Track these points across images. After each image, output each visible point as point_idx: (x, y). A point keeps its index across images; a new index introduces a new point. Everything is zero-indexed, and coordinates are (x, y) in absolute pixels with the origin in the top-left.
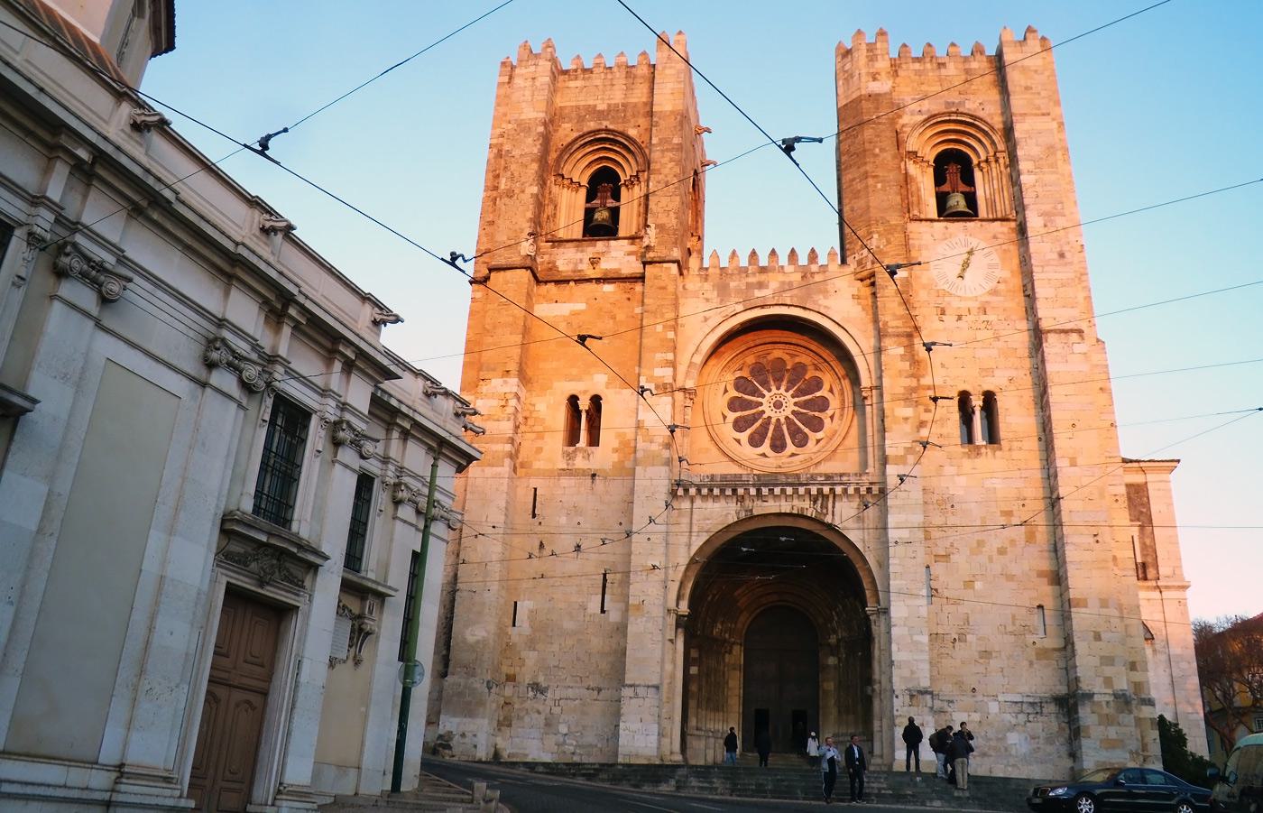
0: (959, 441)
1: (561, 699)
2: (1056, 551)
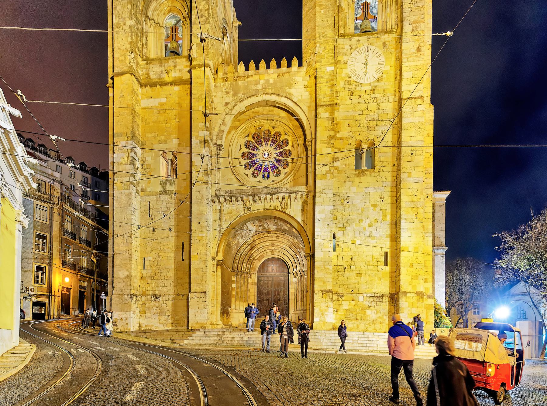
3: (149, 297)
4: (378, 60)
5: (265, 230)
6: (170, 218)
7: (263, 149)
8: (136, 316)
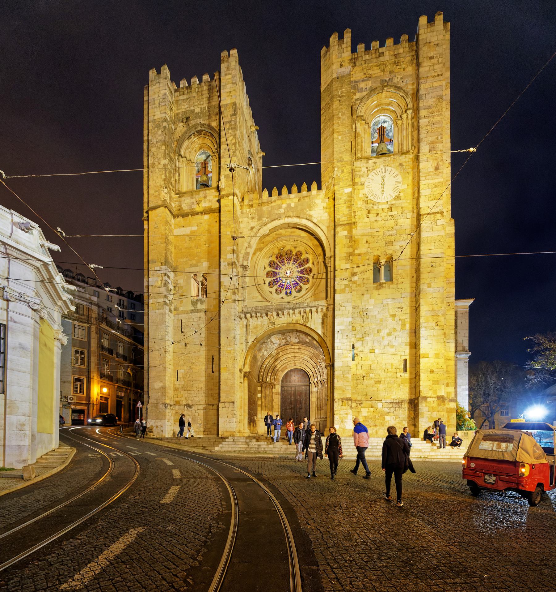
0: (372, 281)
2: (415, 332)
3: (182, 407)
4: (395, 180)
5: (288, 343)
6: (200, 334)
7: (286, 268)
8: (170, 424)
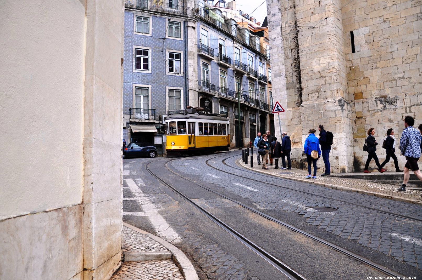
1: (411, 106)
